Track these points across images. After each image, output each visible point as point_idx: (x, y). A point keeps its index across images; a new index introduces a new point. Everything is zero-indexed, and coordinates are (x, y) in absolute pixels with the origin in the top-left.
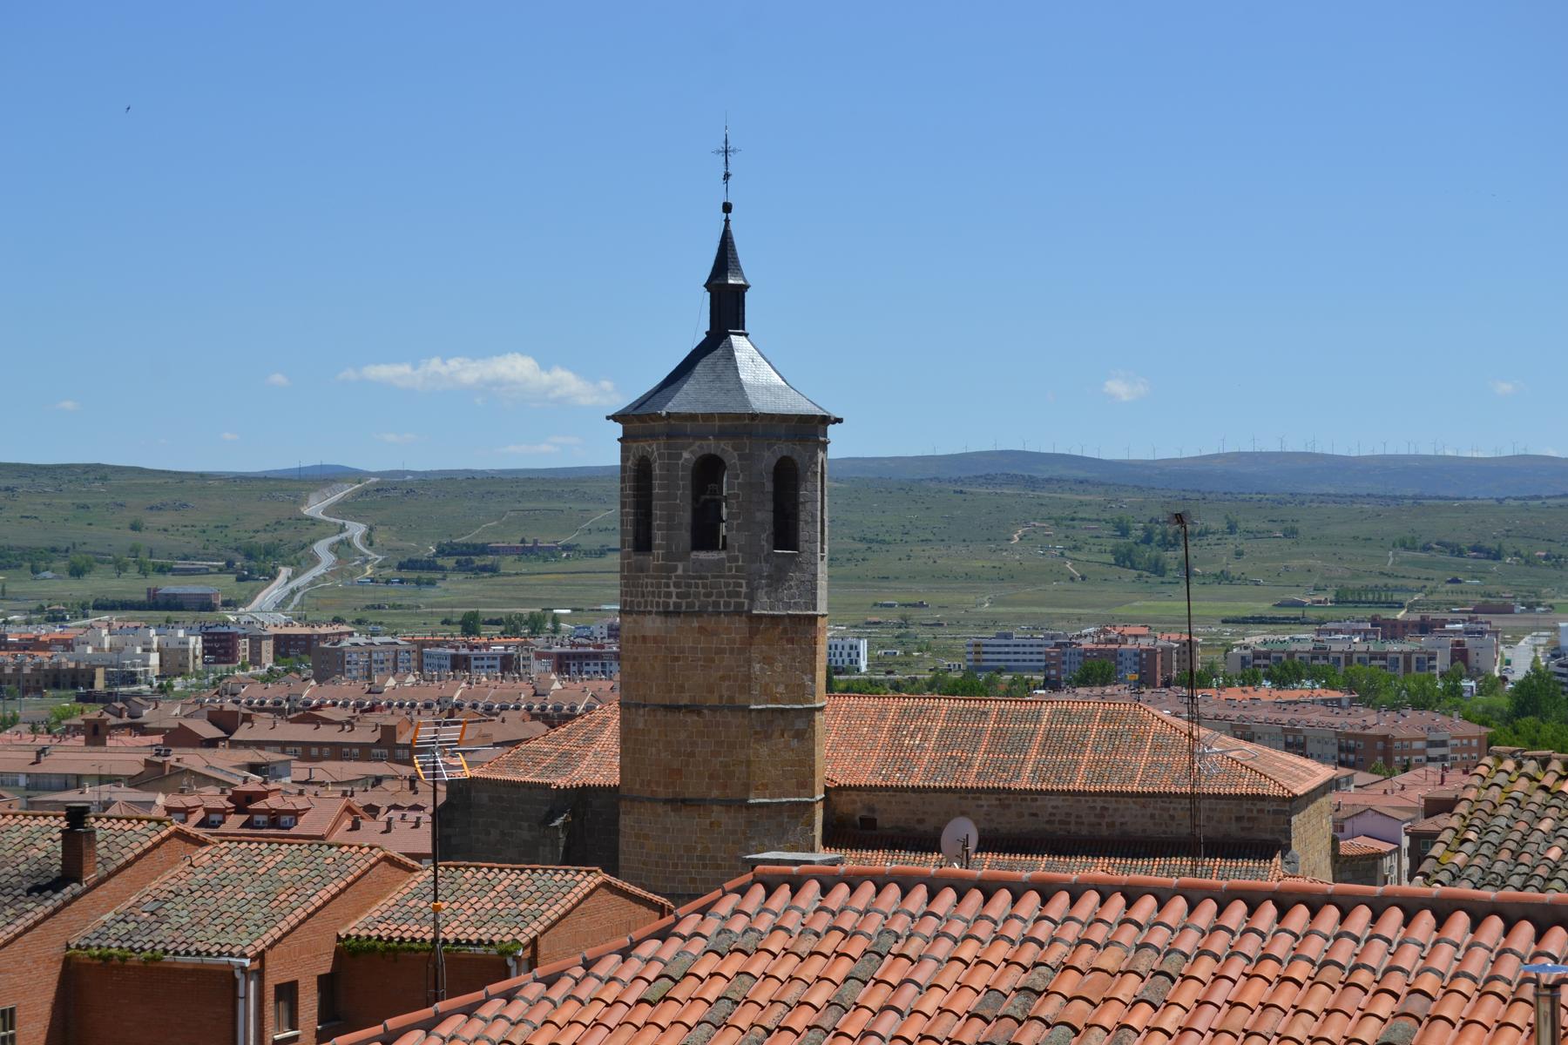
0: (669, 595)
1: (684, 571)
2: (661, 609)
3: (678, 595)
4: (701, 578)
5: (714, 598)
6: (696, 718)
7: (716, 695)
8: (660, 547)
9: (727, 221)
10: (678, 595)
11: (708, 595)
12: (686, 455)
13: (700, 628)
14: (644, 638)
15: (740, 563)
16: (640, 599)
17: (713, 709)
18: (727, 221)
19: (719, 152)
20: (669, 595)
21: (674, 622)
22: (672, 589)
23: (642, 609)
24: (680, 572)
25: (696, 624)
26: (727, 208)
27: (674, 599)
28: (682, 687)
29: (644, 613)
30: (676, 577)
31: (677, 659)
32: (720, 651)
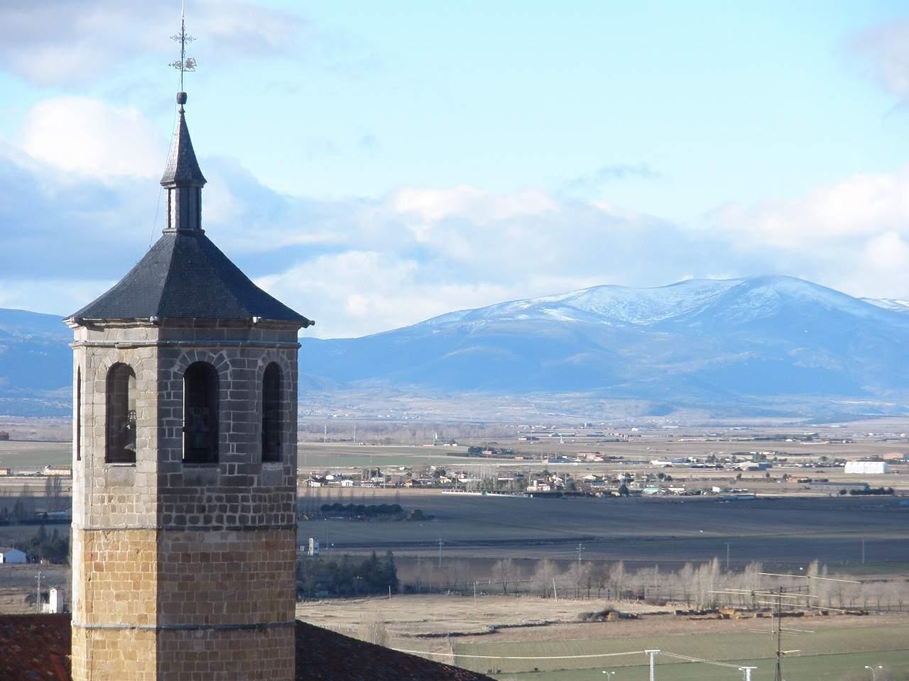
0: (245, 509)
1: (259, 484)
2: (237, 524)
3: (257, 509)
4: (268, 491)
5: (275, 512)
6: (263, 638)
7: (276, 612)
8: (233, 458)
9: (182, 112)
10: (257, 509)
11: (272, 509)
12: (260, 363)
13: (267, 542)
14: (205, 557)
15: (291, 475)
16: (195, 514)
17: (274, 626)
18: (182, 112)
19: (177, 38)
20: (245, 509)
21: (250, 538)
22: (251, 504)
23: (201, 524)
24: (255, 485)
25: (264, 540)
26: (183, 99)
27: (251, 514)
28: (255, 604)
29: (206, 529)
30: (255, 490)
31: (252, 577)
32: (278, 567)
